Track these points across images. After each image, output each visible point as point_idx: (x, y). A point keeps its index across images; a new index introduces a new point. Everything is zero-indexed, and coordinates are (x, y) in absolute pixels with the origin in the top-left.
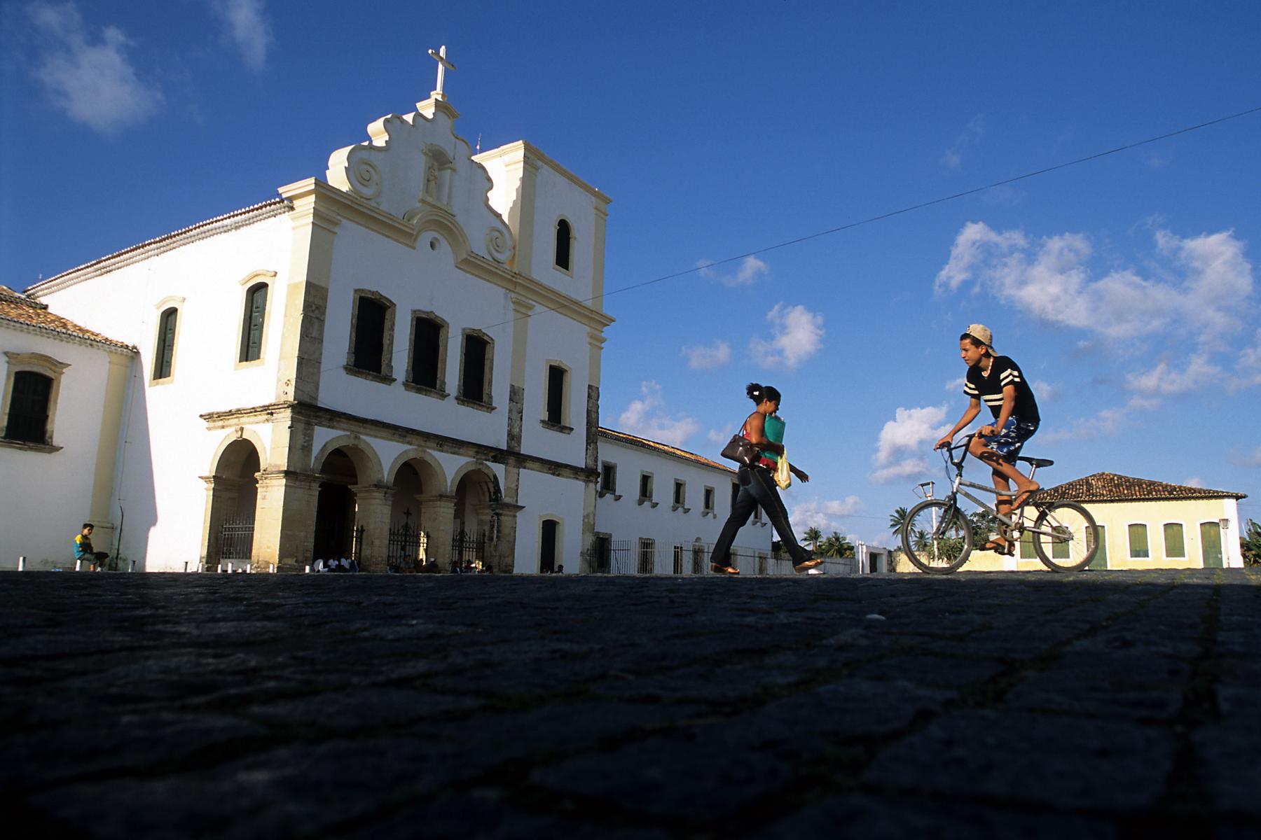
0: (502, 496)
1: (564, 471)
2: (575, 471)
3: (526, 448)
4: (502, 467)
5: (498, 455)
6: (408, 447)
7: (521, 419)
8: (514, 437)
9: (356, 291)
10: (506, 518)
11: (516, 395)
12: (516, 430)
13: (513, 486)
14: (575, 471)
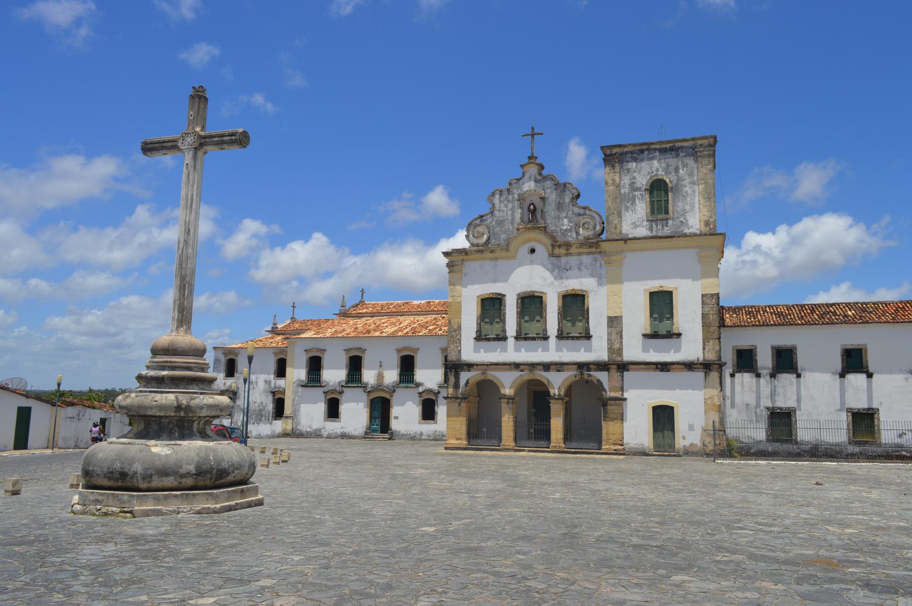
4: (605, 374)
6: (522, 373)
8: (615, 349)
9: (478, 297)
11: (614, 322)
12: (616, 346)
13: (618, 385)
14: (689, 366)
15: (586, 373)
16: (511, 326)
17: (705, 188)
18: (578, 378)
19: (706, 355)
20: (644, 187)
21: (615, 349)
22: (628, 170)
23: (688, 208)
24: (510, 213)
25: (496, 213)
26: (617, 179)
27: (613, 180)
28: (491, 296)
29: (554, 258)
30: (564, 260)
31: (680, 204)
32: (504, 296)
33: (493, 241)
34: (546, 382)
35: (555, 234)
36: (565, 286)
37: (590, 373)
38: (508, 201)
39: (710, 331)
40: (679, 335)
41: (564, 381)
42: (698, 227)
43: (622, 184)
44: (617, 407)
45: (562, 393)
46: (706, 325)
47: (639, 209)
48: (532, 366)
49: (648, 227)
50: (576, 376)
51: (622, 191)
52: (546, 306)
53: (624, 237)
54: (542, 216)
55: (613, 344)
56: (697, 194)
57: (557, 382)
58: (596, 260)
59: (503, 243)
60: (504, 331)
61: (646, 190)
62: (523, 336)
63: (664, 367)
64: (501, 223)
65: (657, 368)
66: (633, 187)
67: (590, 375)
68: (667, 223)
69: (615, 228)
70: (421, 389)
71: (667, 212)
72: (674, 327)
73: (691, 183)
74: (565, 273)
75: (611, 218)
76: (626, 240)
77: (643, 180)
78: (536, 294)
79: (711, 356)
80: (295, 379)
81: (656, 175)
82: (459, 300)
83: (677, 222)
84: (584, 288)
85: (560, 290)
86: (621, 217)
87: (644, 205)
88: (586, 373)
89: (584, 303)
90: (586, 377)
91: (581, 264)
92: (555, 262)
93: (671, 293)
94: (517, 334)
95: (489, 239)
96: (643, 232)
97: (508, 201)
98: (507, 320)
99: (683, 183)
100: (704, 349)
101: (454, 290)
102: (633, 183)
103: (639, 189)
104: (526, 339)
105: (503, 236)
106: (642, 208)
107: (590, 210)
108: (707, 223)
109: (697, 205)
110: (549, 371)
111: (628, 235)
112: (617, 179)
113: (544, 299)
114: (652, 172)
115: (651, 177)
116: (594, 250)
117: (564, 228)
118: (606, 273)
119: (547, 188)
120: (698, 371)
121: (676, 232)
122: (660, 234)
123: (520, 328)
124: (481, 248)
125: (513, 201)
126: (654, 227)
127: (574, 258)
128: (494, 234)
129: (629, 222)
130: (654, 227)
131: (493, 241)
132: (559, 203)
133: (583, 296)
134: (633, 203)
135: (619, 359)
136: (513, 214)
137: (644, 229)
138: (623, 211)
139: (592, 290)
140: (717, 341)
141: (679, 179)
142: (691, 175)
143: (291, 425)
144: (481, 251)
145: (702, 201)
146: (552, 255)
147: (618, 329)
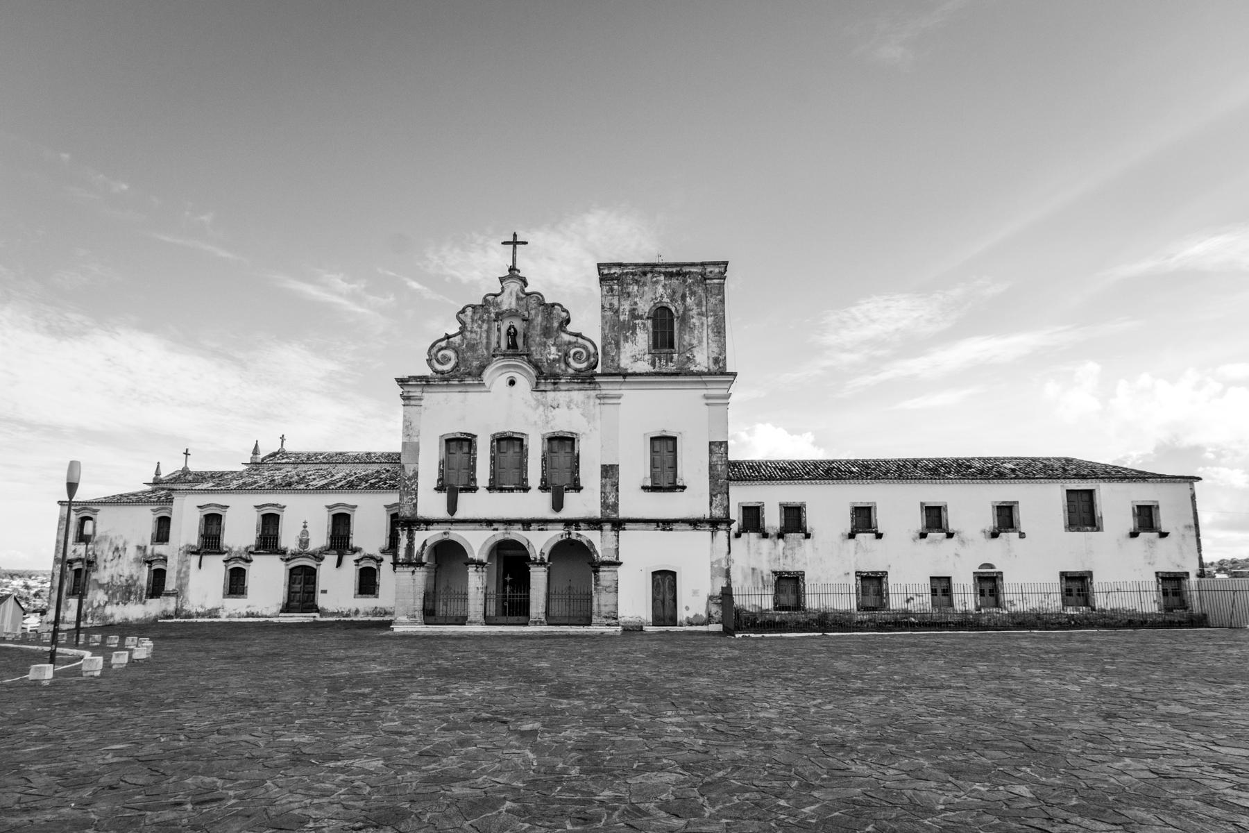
0: (598, 556)
1: (675, 526)
2: (695, 523)
3: (623, 513)
4: (599, 532)
5: (595, 524)
7: (617, 490)
8: (609, 505)
10: (605, 573)
11: (609, 472)
12: (611, 500)
13: (613, 546)
14: (695, 523)
15: (574, 533)
16: (483, 474)
17: (714, 321)
18: (564, 538)
19: (713, 511)
20: (646, 315)
21: (609, 505)
22: (629, 294)
23: (695, 342)
24: (484, 335)
25: (468, 335)
26: (616, 302)
27: (611, 304)
28: (459, 436)
29: (539, 393)
30: (550, 395)
31: (687, 337)
32: (476, 436)
33: (462, 368)
34: (525, 544)
35: (540, 364)
36: (552, 428)
37: (579, 532)
38: (483, 321)
39: (717, 484)
40: (684, 488)
41: (547, 542)
42: (706, 365)
43: (621, 310)
44: (608, 573)
45: (546, 557)
46: (713, 477)
47: (640, 340)
48: (509, 522)
49: (650, 361)
50: (562, 536)
51: (622, 318)
52: (527, 450)
53: (622, 372)
54: (524, 342)
55: (607, 498)
56: (705, 327)
57: (539, 542)
58: (588, 397)
59: (475, 371)
60: (474, 480)
61: (648, 318)
62: (498, 486)
63: (666, 524)
64: (472, 347)
65: (658, 526)
66: (634, 314)
67: (579, 535)
68: (672, 358)
69: (613, 360)
70: (357, 556)
71: (672, 345)
72: (678, 480)
73: (699, 314)
74: (551, 412)
75: (608, 348)
76: (625, 375)
77: (644, 307)
78: (515, 436)
79: (718, 513)
80: (182, 544)
81: (661, 302)
82: (415, 440)
83: (683, 358)
84: (574, 432)
85: (544, 432)
86: (619, 349)
87: (646, 336)
88: (574, 533)
89: (573, 448)
90: (574, 537)
91: (571, 401)
92: (539, 397)
93: (674, 439)
94: (490, 483)
95: (457, 365)
96: (644, 366)
97: (483, 321)
98: (477, 467)
99: (691, 313)
100: (711, 504)
101: (410, 427)
102: (634, 309)
103: (641, 317)
104: (502, 490)
105: (475, 363)
106: (644, 338)
107: (583, 338)
108: (716, 361)
109: (705, 339)
110: (529, 530)
111: (627, 369)
112: (616, 302)
113: (525, 443)
114: (656, 298)
115: (655, 304)
116: (587, 386)
117: (551, 357)
118: (601, 413)
119: (532, 309)
120: (704, 530)
121: (681, 369)
122: (664, 371)
123: (494, 476)
124: (446, 375)
125: (489, 321)
126: (657, 361)
127: (563, 393)
128: (465, 360)
129: (629, 354)
130: (657, 361)
131: (462, 368)
132: (547, 328)
133: (573, 440)
134: (634, 333)
135: (614, 516)
136: (488, 337)
137: (646, 364)
138: (622, 342)
139: (584, 433)
140: (726, 496)
141: (686, 309)
142: (699, 304)
143: (175, 605)
144: (448, 380)
145: (711, 335)
146: (536, 388)
147: (614, 480)
